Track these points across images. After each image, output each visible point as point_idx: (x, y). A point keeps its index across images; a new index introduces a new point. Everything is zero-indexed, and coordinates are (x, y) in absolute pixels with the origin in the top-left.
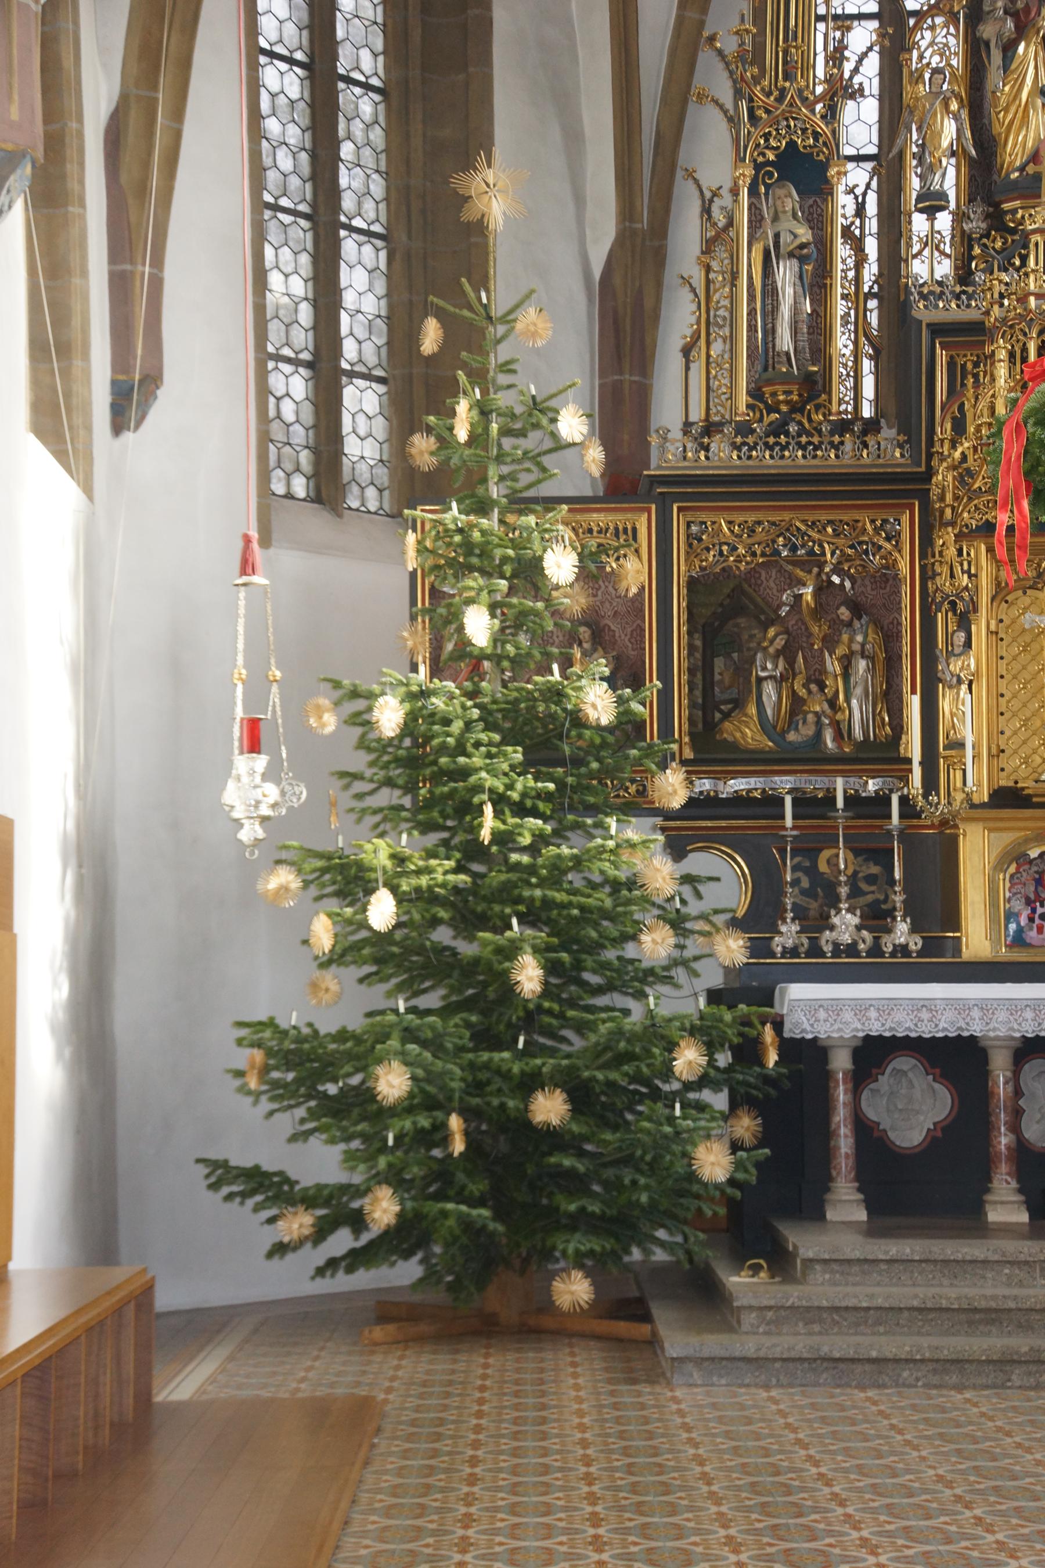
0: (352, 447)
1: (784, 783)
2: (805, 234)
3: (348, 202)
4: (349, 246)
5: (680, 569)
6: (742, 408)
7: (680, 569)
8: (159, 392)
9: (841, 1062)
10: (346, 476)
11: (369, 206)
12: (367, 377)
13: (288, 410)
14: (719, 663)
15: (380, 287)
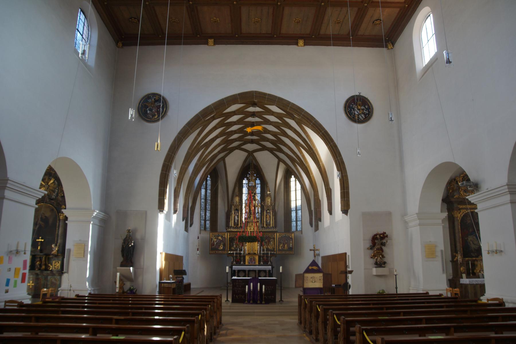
0: (207, 226)
1: (235, 252)
2: (238, 214)
3: (207, 208)
4: (207, 211)
5: (228, 237)
6: (233, 226)
7: (228, 237)
8: (193, 224)
9: (236, 271)
10: (206, 228)
11: (209, 208)
12: (208, 220)
13: (202, 224)
14: (231, 244)
15: (210, 214)
